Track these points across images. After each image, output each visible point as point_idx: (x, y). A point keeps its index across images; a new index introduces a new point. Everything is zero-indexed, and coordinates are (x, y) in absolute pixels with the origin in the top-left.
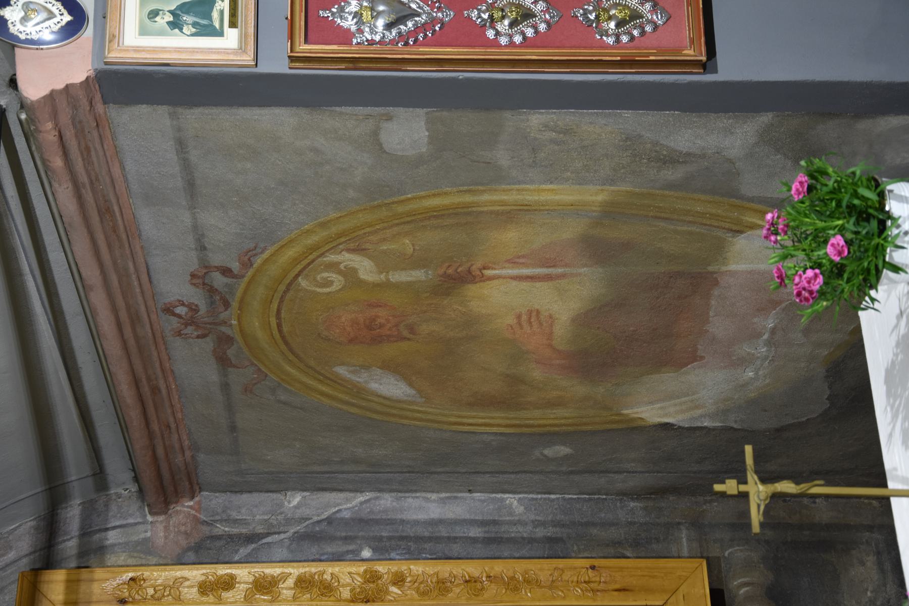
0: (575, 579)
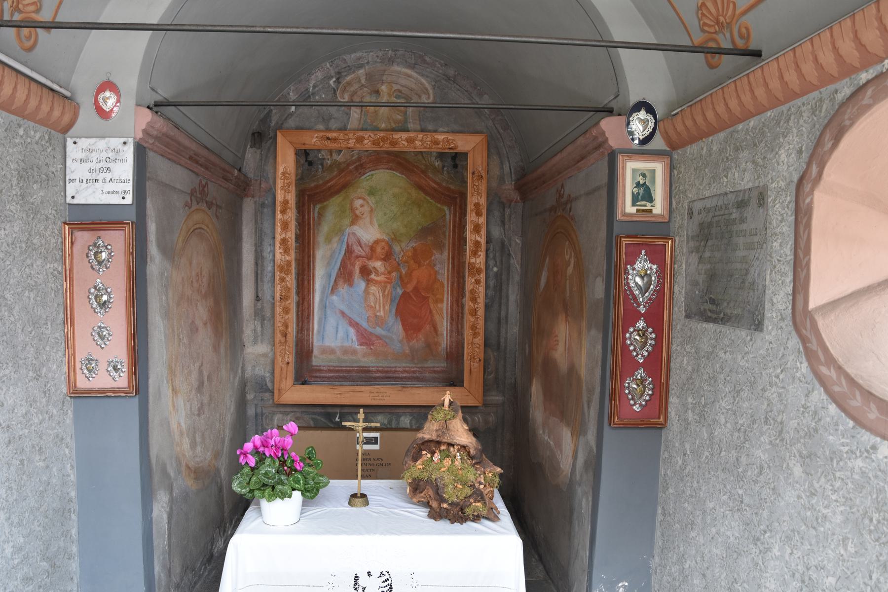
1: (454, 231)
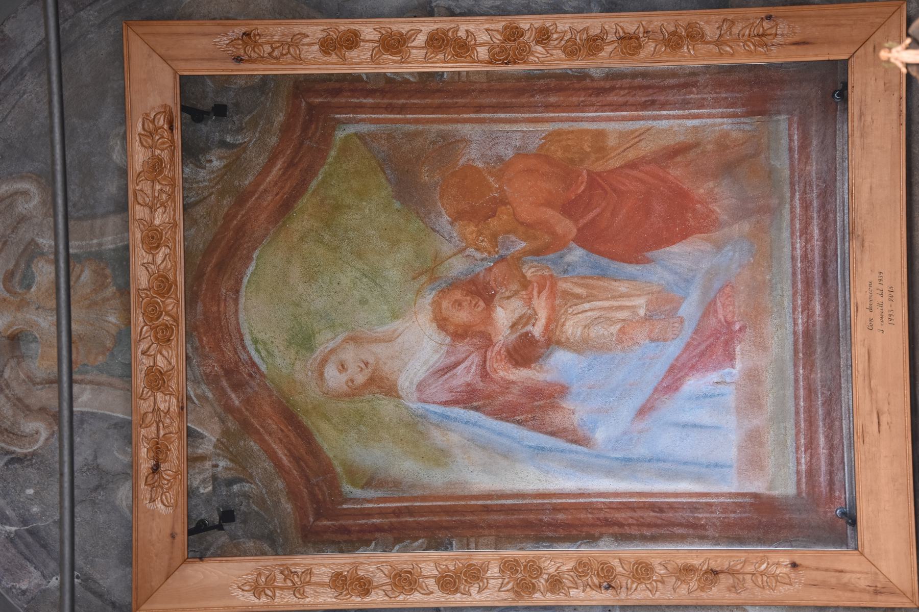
0: (747, 32)
1: (402, 109)
